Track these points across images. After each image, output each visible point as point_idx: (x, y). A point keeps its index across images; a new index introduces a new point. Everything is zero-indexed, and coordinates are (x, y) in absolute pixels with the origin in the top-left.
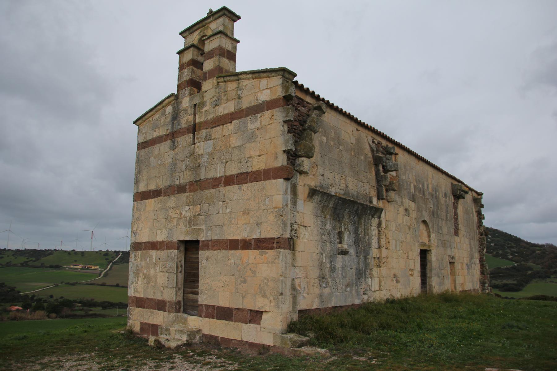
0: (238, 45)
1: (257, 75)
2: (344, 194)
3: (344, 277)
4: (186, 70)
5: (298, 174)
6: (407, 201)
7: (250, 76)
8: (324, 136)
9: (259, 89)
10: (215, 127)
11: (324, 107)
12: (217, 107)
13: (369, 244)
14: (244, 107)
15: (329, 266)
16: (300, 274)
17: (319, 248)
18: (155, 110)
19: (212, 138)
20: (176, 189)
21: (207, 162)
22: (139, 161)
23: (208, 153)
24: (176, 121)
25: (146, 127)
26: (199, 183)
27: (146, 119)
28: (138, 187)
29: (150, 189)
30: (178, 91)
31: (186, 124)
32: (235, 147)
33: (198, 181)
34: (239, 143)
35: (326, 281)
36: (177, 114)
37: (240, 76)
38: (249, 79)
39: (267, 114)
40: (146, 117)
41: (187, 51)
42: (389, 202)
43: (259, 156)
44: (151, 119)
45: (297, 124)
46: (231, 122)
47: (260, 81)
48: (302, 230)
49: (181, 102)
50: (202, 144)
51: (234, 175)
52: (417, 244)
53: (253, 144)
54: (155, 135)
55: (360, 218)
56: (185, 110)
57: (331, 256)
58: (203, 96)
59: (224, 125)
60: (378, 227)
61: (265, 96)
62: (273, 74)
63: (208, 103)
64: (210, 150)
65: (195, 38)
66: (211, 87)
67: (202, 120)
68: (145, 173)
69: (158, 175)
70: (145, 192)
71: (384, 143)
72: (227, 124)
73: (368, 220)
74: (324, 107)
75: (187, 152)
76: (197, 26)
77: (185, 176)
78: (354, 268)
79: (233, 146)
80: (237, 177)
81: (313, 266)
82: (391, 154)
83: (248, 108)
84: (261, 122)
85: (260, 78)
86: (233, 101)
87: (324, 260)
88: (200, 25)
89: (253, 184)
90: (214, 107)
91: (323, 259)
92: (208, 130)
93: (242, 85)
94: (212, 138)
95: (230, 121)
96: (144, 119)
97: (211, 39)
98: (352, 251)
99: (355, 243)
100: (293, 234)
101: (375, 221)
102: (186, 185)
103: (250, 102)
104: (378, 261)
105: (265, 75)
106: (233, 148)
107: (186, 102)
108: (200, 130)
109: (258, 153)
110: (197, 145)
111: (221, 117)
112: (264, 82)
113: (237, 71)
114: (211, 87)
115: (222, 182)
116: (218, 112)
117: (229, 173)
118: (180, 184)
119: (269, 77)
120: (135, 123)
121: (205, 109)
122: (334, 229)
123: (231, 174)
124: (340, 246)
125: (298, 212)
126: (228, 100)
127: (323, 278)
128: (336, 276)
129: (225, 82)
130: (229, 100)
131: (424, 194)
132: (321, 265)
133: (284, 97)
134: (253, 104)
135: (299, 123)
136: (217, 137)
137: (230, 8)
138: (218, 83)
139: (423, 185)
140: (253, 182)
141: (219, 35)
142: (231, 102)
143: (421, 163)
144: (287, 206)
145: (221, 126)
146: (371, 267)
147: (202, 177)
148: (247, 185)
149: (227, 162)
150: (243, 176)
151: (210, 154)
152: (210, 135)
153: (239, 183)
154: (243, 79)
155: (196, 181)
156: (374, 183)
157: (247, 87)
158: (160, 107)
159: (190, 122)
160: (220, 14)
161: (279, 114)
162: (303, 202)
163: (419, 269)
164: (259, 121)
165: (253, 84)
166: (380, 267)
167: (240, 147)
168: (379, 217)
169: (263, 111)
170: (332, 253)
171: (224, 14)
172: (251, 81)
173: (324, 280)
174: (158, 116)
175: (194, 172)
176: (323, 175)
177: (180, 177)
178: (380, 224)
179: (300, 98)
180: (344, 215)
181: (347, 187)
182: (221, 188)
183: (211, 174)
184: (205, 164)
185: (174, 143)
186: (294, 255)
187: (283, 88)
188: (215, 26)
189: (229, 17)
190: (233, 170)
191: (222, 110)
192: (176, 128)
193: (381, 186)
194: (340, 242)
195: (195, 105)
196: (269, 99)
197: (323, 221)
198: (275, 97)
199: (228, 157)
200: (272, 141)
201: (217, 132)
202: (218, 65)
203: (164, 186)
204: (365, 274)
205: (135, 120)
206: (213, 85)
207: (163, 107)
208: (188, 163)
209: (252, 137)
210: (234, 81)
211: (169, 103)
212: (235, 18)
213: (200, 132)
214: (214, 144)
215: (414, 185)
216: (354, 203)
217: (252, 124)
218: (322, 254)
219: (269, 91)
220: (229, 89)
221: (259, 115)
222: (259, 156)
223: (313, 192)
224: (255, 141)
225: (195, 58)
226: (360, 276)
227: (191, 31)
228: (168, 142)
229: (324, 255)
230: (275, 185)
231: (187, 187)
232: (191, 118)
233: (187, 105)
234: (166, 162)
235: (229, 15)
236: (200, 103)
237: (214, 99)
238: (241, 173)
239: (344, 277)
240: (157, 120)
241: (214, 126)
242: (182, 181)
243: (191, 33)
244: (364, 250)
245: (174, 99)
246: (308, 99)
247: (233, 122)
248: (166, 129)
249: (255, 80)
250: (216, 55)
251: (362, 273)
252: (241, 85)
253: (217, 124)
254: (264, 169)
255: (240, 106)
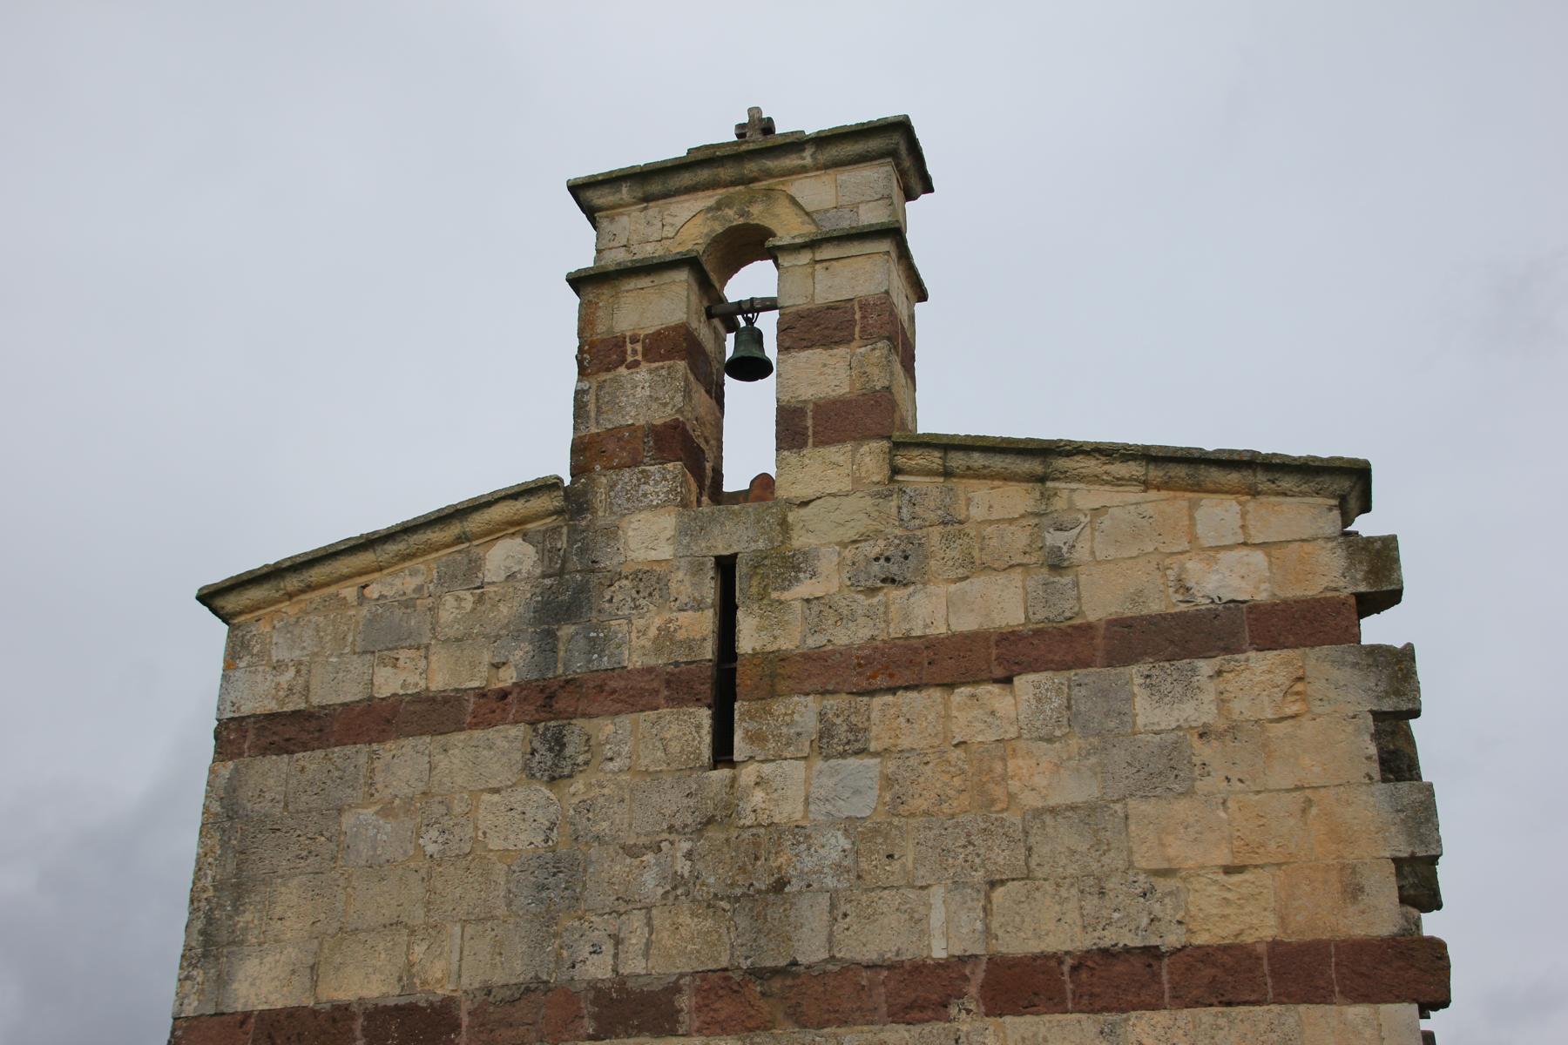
0: (919, 307)
1: (1180, 471)
4: (642, 374)
7: (1134, 469)
9: (1193, 538)
10: (892, 690)
12: (895, 594)
14: (1095, 612)
18: (392, 548)
19: (873, 746)
20: (587, 1008)
21: (838, 868)
22: (226, 817)
23: (849, 825)
24: (566, 631)
25: (288, 635)
26: (776, 985)
27: (310, 588)
28: (222, 981)
29: (342, 996)
30: (576, 471)
31: (658, 650)
32: (1053, 811)
33: (776, 972)
34: (1076, 790)
36: (583, 589)
37: (1062, 463)
38: (1118, 482)
39: (1261, 671)
40: (316, 574)
41: (644, 282)
43: (1228, 870)
44: (349, 592)
46: (1007, 681)
47: (1193, 506)
49: (611, 533)
50: (795, 770)
51: (1058, 958)
53: (1182, 807)
54: (388, 683)
56: (650, 581)
58: (784, 524)
59: (950, 686)
61: (1234, 578)
62: (1287, 483)
63: (827, 562)
64: (864, 806)
65: (687, 222)
66: (846, 485)
67: (786, 643)
68: (290, 895)
69: (418, 916)
70: (291, 1013)
72: (977, 682)
75: (671, 801)
76: (704, 174)
77: (665, 938)
79: (1031, 800)
80: (1074, 969)
83: (1121, 625)
84: (1222, 700)
85: (1198, 488)
86: (1017, 575)
88: (726, 173)
89: (1205, 1015)
90: (872, 591)
92: (831, 702)
93: (1071, 507)
94: (873, 746)
95: (999, 672)
96: (292, 583)
97: (826, 252)
102: (675, 989)
103: (1137, 596)
105: (1234, 477)
106: (1038, 813)
107: (649, 533)
108: (773, 694)
109: (1223, 856)
110: (747, 774)
111: (932, 644)
112: (1219, 514)
113: (920, 431)
114: (846, 485)
115: (973, 989)
116: (906, 617)
117: (1016, 944)
118: (621, 981)
119: (1254, 493)
120: (209, 597)
121: (805, 588)
123: (1034, 947)
126: (972, 567)
129: (947, 474)
130: (986, 568)
133: (1359, 597)
134: (1155, 607)
136: (905, 743)
137: (919, 134)
138: (896, 471)
140: (1197, 1003)
141: (886, 245)
142: (1001, 579)
145: (936, 694)
147: (811, 950)
148: (1161, 1017)
149: (993, 884)
150: (1120, 967)
151: (860, 832)
152: (852, 729)
153: (1091, 1003)
154: (1081, 478)
155: (757, 973)
157: (1106, 522)
158: (435, 536)
159: (689, 644)
160: (874, 144)
161: (1342, 675)
164: (1209, 695)
165: (1149, 509)
167: (1087, 813)
169: (1227, 650)
171: (892, 154)
172: (1133, 495)
174: (411, 583)
175: (743, 922)
177: (617, 941)
182: (967, 1022)
183: (878, 938)
184: (830, 882)
185: (558, 744)
187: (1350, 557)
188: (819, 193)
190: (1048, 927)
191: (929, 611)
192: (573, 659)
195: (726, 567)
196: (1262, 596)
198: (1313, 589)
199: (1002, 856)
200: (1309, 802)
201: (909, 717)
202: (888, 389)
203: (472, 980)
205: (218, 575)
206: (856, 481)
207: (459, 540)
208: (683, 867)
209: (1169, 769)
210: (1008, 477)
211: (515, 526)
212: (915, 183)
213: (778, 707)
214: (888, 781)
217: (1157, 706)
219: (1258, 557)
220: (977, 513)
221: (1205, 667)
222: (1228, 870)
224: (1189, 793)
225: (694, 325)
227: (655, 187)
228: (509, 740)
230: (1368, 1033)
231: (684, 1001)
232: (704, 624)
233: (665, 552)
234: (495, 843)
235: (907, 163)
236: (758, 562)
237: (871, 549)
238: (1105, 952)
240: (408, 604)
241: (881, 681)
242: (634, 965)
243: (647, 199)
245: (561, 513)
247: (1023, 682)
248: (487, 657)
249: (1153, 494)
250: (868, 338)
252: (1059, 504)
253: (907, 676)
254: (1274, 944)
255: (1068, 606)
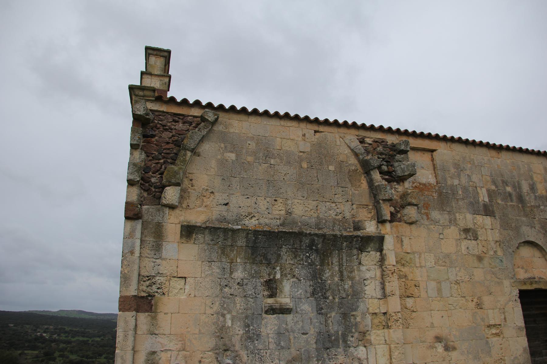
2: (282, 225)
3: (283, 348)
5: (167, 210)
6: (469, 216)
8: (232, 152)
11: (210, 116)
13: (357, 294)
15: (241, 332)
16: (171, 346)
17: (216, 307)
35: (233, 354)
42: (411, 223)
45: (171, 146)
48: (178, 284)
52: (507, 283)
55: (324, 256)
57: (247, 317)
60: (381, 266)
71: (391, 139)
73: (350, 255)
74: (210, 116)
78: (312, 331)
81: (200, 332)
82: (405, 152)
87: (229, 323)
91: (225, 321)
98: (307, 307)
99: (313, 294)
100: (156, 290)
101: (370, 258)
104: (383, 318)
122: (253, 277)
124: (270, 301)
125: (165, 259)
127: (226, 350)
128: (260, 347)
131: (521, 199)
132: (221, 332)
135: (175, 145)
139: (517, 187)
143: (504, 155)
144: (132, 253)
146: (361, 328)
156: (366, 199)
162: (176, 245)
163: (520, 322)
166: (388, 327)
168: (381, 250)
170: (249, 312)
173: (229, 353)
176: (226, 204)
178: (382, 260)
179: (175, 115)
180: (279, 256)
181: (289, 213)
186: (154, 318)
189: (156, 55)
193: (378, 202)
194: (271, 296)
197: (227, 266)
204: (345, 341)
215: (488, 191)
216: (300, 235)
218: (223, 315)
223: (188, 231)
226: (328, 345)
229: (228, 316)
235: (155, 53)
239: (283, 348)
244: (340, 303)
246: (197, 112)
251: (337, 340)
